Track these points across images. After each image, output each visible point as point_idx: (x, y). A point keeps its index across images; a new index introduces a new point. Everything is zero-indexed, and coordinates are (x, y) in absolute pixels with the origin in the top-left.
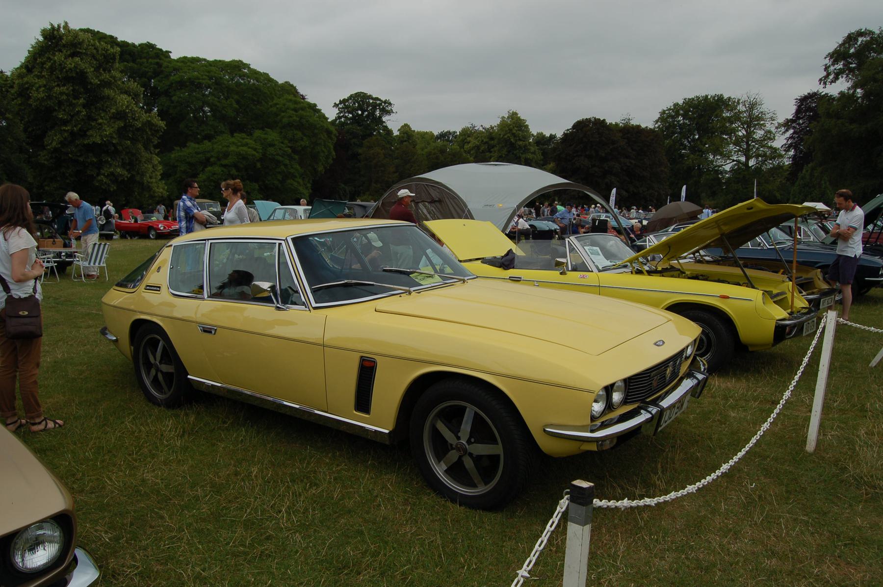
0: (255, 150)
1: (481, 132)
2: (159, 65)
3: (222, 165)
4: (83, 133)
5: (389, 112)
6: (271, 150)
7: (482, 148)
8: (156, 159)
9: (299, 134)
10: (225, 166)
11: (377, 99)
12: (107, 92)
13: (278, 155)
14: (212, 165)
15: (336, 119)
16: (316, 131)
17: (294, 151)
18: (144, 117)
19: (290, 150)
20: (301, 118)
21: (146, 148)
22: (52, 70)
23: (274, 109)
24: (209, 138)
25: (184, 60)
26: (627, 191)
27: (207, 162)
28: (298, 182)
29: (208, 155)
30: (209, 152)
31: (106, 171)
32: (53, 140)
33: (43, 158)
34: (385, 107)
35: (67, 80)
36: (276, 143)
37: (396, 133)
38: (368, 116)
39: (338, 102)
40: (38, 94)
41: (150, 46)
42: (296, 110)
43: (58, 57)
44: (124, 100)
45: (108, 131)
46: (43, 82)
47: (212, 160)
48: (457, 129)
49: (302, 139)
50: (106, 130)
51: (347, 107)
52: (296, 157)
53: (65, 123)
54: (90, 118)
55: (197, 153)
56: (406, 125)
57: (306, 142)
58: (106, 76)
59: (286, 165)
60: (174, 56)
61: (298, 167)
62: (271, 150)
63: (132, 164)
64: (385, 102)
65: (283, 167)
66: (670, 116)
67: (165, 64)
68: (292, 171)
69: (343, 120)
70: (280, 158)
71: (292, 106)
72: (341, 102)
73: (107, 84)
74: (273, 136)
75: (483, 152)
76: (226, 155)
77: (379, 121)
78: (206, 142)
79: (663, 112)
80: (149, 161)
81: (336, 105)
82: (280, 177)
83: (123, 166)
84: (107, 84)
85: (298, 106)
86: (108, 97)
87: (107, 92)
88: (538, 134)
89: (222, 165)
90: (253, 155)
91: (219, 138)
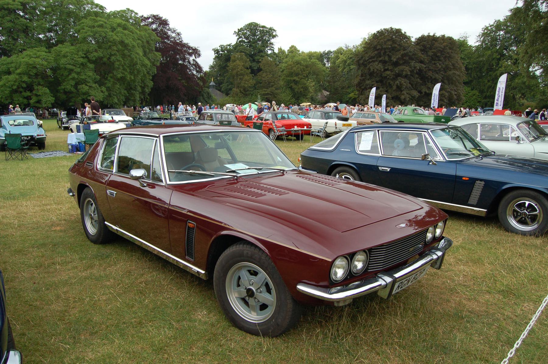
0: (46, 60)
1: (350, 50)
5: (274, 37)
7: (348, 62)
10: (20, 74)
11: (263, 27)
26: (420, 92)
27: (9, 73)
28: (90, 87)
30: (12, 63)
34: (270, 33)
36: (69, 54)
39: (237, 31)
48: (333, 49)
49: (96, 51)
51: (244, 34)
52: (92, 66)
56: (292, 47)
57: (100, 54)
59: (78, 73)
61: (91, 73)
62: (63, 61)
66: (492, 31)
70: (71, 67)
72: (239, 30)
75: (349, 65)
77: (266, 44)
79: (487, 28)
82: (73, 83)
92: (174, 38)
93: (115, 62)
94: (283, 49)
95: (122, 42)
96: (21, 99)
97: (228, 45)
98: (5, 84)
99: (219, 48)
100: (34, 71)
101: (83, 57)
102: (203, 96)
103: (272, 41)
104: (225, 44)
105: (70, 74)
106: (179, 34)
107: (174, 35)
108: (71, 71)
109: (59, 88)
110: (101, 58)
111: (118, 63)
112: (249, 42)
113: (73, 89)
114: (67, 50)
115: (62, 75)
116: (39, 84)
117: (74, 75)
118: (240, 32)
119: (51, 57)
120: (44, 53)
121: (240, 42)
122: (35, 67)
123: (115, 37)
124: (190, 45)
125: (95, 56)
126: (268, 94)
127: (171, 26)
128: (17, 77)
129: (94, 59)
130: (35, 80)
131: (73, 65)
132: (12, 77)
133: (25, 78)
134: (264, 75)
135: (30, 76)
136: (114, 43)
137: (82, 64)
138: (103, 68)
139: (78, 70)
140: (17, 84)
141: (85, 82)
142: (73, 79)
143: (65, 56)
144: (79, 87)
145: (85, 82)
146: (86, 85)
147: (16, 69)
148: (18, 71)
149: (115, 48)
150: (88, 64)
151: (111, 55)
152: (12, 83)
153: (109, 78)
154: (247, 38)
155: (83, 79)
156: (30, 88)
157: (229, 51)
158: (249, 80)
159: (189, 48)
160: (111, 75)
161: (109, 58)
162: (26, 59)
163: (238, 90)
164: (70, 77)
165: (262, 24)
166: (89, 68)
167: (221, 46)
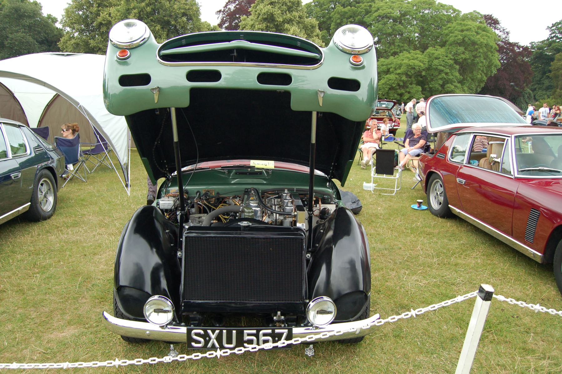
0: (422, 62)
2: (370, 6)
3: (396, 74)
6: (436, 62)
9: (462, 49)
10: (399, 74)
13: (441, 65)
14: (391, 73)
15: (548, 39)
16: (476, 47)
17: (456, 62)
19: (451, 62)
23: (446, 31)
24: (395, 54)
28: (455, 86)
29: (389, 67)
36: (441, 57)
39: (551, 26)
42: (462, 31)
47: (391, 70)
49: (463, 53)
52: (457, 67)
55: (382, 65)
57: (467, 55)
59: (447, 74)
61: (457, 74)
62: (436, 62)
65: (443, 75)
67: (373, 5)
68: (451, 77)
69: (554, 39)
70: (442, 68)
71: (460, 28)
74: (440, 51)
76: (400, 66)
78: (392, 58)
82: (441, 82)
85: (464, 28)
86: (287, 29)
88: (49, 17)
89: (396, 74)
90: (420, 66)
91: (401, 54)
92: (500, 36)
93: (478, 63)
95: (487, 45)
96: (396, 95)
97: (541, 42)
98: (386, 82)
99: (529, 45)
100: (413, 72)
101: (451, 59)
102: (524, 96)
104: (536, 41)
105: (440, 74)
106: (508, 33)
107: (500, 34)
108: (442, 71)
109: (427, 86)
110: (465, 59)
111: (481, 64)
113: (440, 88)
114: (439, 52)
115: (432, 75)
116: (411, 84)
117: (443, 75)
119: (426, 60)
120: (420, 56)
121: (552, 38)
122: (414, 68)
123: (482, 40)
124: (520, 44)
125: (462, 58)
128: (397, 76)
129: (461, 60)
130: (409, 79)
131: (443, 66)
132: (392, 76)
133: (404, 78)
135: (407, 75)
136: (481, 45)
137: (450, 66)
138: (465, 68)
139: (448, 71)
140: (396, 82)
141: (451, 82)
142: (441, 79)
143: (436, 58)
144: (446, 87)
145: (451, 82)
146: (452, 84)
147: (396, 69)
148: (399, 71)
149: (481, 51)
150: (455, 65)
151: (475, 57)
152: (393, 81)
153: (468, 78)
155: (449, 79)
156: (404, 86)
159: (519, 47)
160: (470, 75)
161: (473, 60)
162: (406, 61)
164: (440, 77)
166: (455, 69)
167: (531, 43)
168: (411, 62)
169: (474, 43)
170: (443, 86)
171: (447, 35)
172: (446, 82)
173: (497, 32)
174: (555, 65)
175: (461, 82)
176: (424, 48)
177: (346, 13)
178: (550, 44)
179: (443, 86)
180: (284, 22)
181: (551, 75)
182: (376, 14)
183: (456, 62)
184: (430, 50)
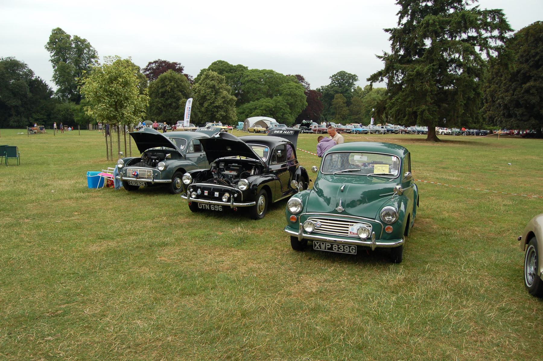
2: (242, 74)
4: (213, 102)
5: (356, 80)
6: (279, 104)
8: (235, 109)
9: (290, 97)
12: (221, 90)
15: (331, 84)
17: (288, 104)
18: (230, 97)
20: (291, 91)
21: (231, 106)
22: (207, 84)
24: (258, 99)
25: (253, 71)
27: (256, 109)
31: (219, 113)
32: (206, 105)
33: (203, 109)
35: (210, 87)
37: (363, 90)
38: (346, 82)
40: (202, 92)
41: (240, 66)
42: (289, 88)
43: (208, 81)
44: (225, 92)
45: (220, 102)
46: (204, 88)
50: (219, 102)
51: (336, 78)
53: (209, 100)
54: (216, 98)
57: (293, 101)
58: (220, 85)
60: (249, 69)
62: (279, 104)
63: (226, 111)
64: (354, 75)
73: (221, 88)
74: (280, 98)
77: (351, 85)
78: (256, 101)
80: (232, 110)
81: (330, 77)
83: (224, 112)
84: (221, 88)
87: (221, 90)
94: (360, 87)
103: (355, 83)
112: (339, 83)
118: (334, 77)
126: (356, 119)
127: (306, 80)
134: (355, 107)
135: (265, 110)
141: (286, 113)
151: (296, 101)
154: (338, 81)
157: (326, 90)
158: (346, 110)
163: (339, 116)
165: (349, 72)
168: (268, 104)
169: (295, 95)
170: (283, 115)
171: (282, 90)
172: (284, 113)
173: (303, 84)
174: (334, 101)
175: (291, 113)
176: (271, 96)
177: (229, 77)
178: (332, 87)
179: (283, 115)
180: (219, 89)
181: (333, 106)
182: (246, 79)
183: (288, 104)
184: (275, 98)
